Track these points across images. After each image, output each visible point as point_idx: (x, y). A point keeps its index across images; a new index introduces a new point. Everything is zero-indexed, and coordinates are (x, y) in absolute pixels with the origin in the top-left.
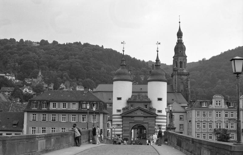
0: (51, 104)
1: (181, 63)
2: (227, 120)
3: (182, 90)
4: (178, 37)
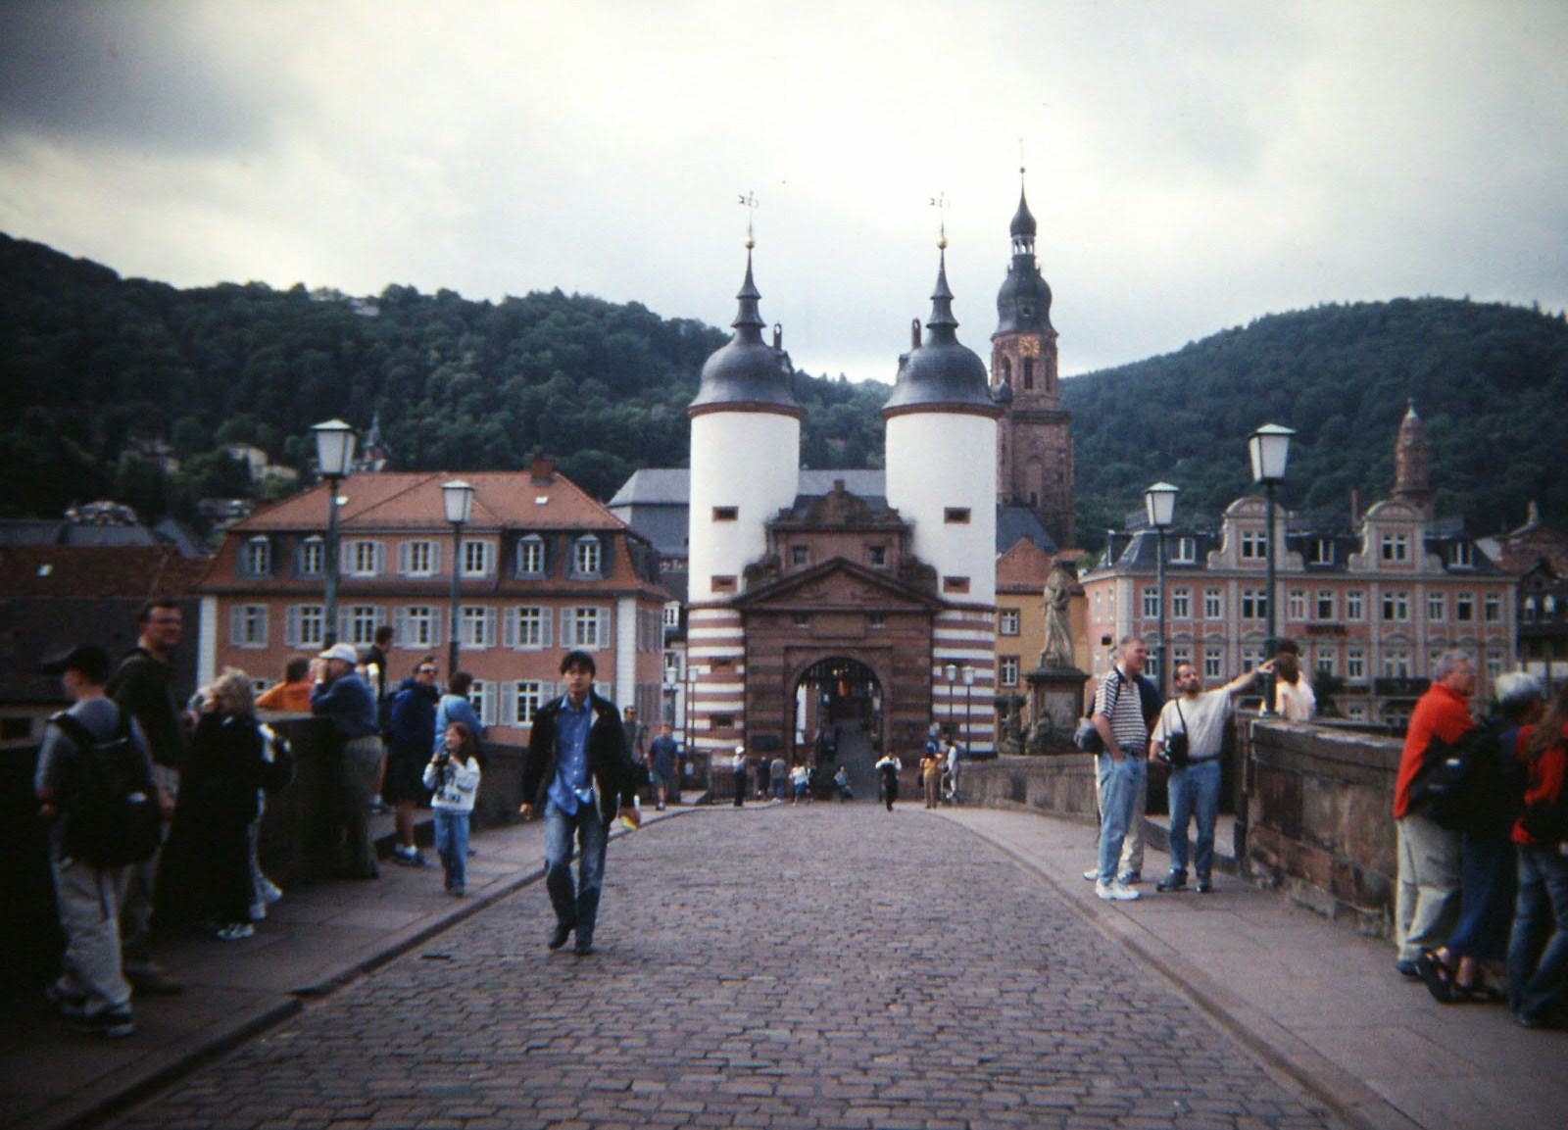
0: (348, 551)
3: (1034, 496)
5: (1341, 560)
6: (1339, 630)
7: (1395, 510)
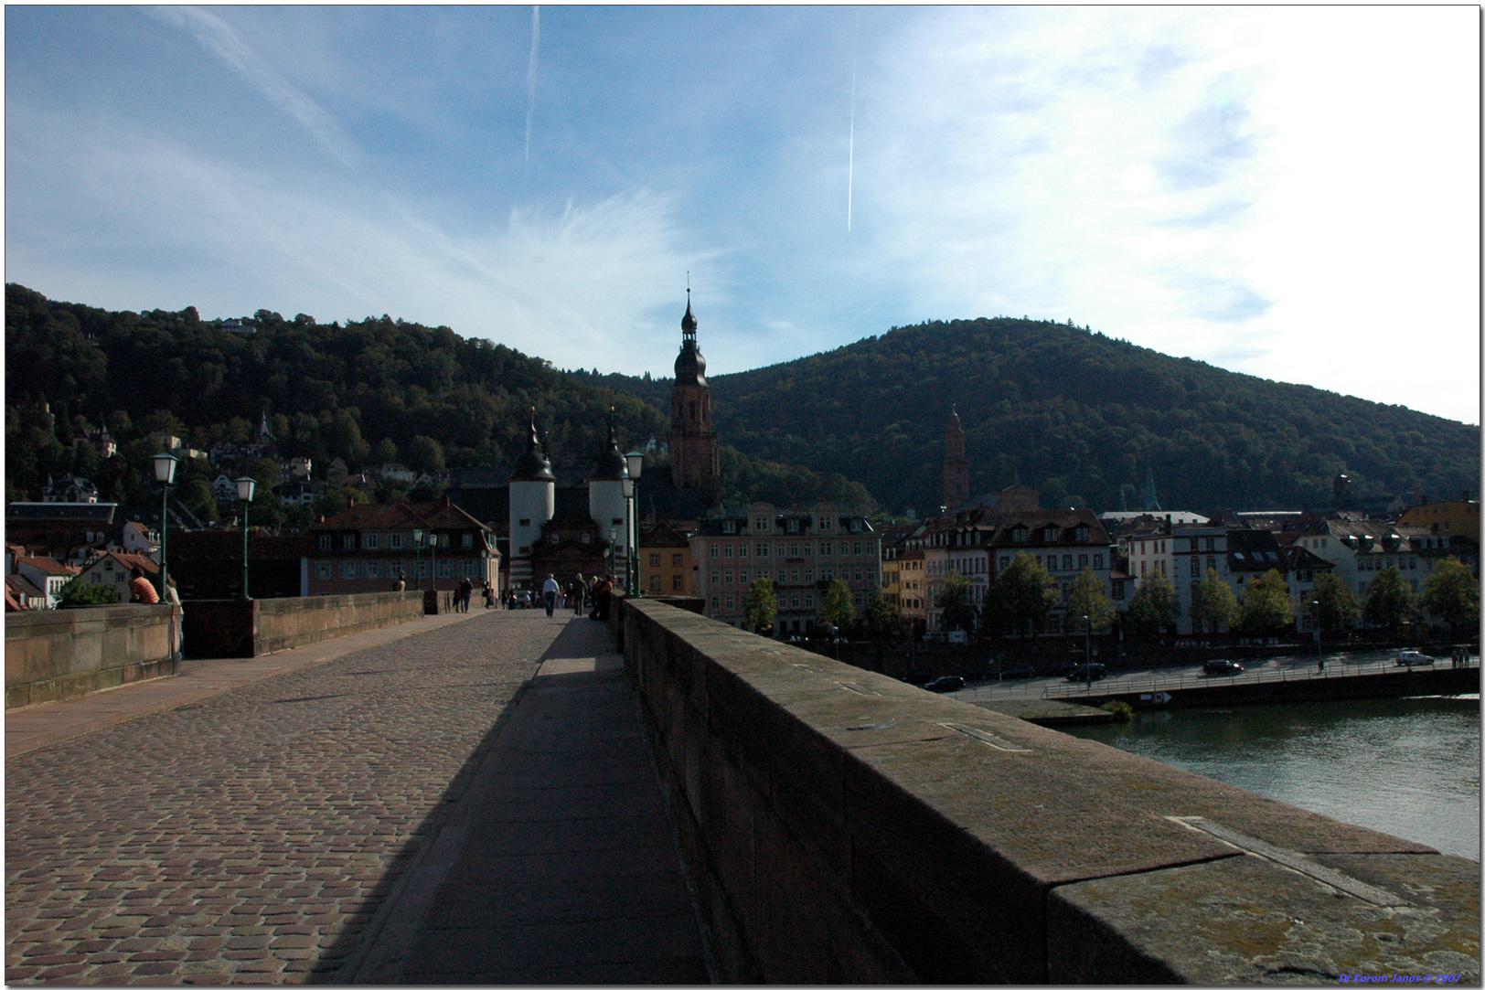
1: (692, 405)
5: (802, 530)
6: (801, 560)
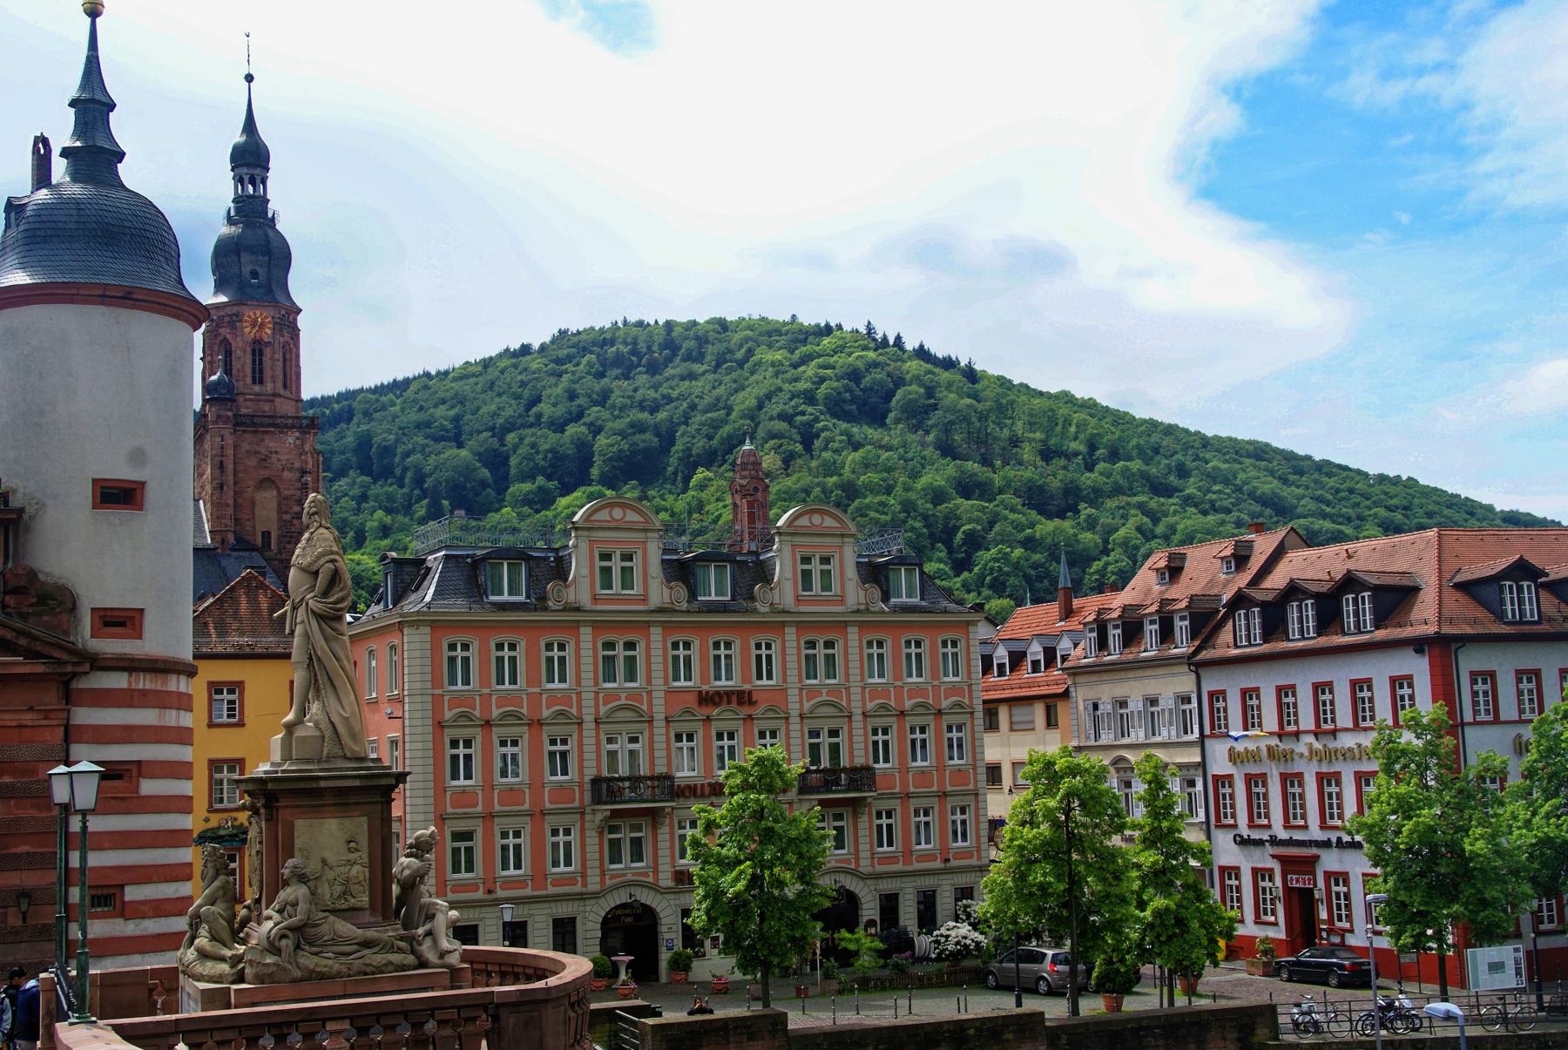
1: (258, 349)
2: (692, 700)
3: (266, 535)
4: (239, 180)
6: (743, 698)
7: (817, 519)
